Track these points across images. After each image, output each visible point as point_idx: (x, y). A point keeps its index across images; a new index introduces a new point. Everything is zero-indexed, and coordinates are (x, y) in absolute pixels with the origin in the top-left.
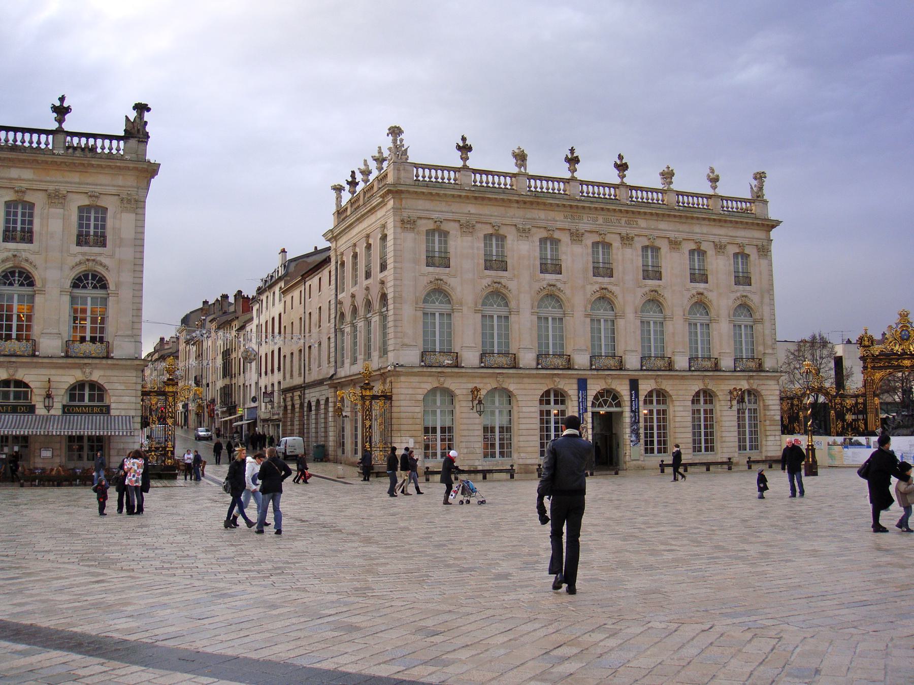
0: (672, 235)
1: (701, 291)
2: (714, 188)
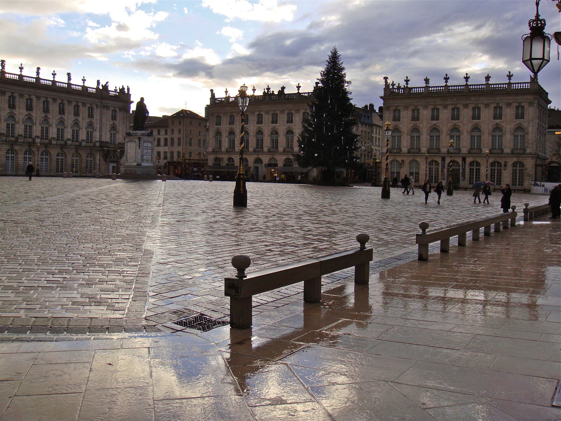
0: (486, 102)
1: (497, 123)
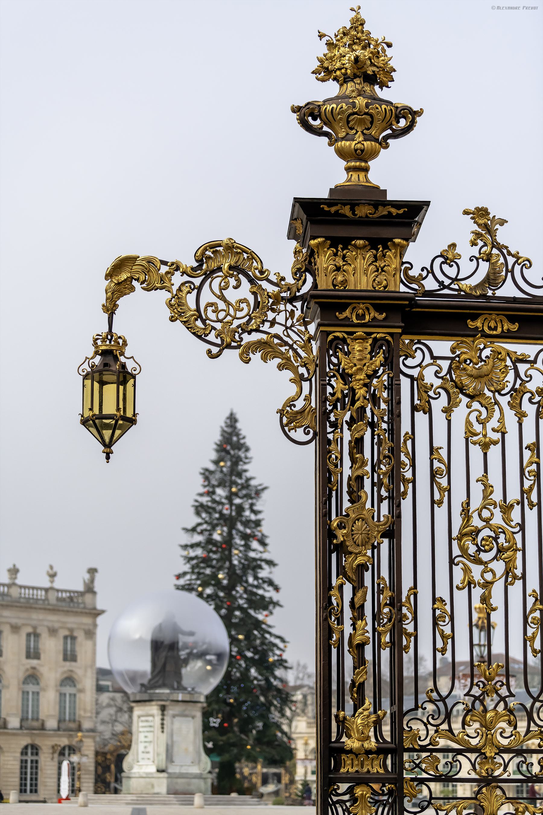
0: (14, 621)
1: (33, 665)
2: (52, 582)
